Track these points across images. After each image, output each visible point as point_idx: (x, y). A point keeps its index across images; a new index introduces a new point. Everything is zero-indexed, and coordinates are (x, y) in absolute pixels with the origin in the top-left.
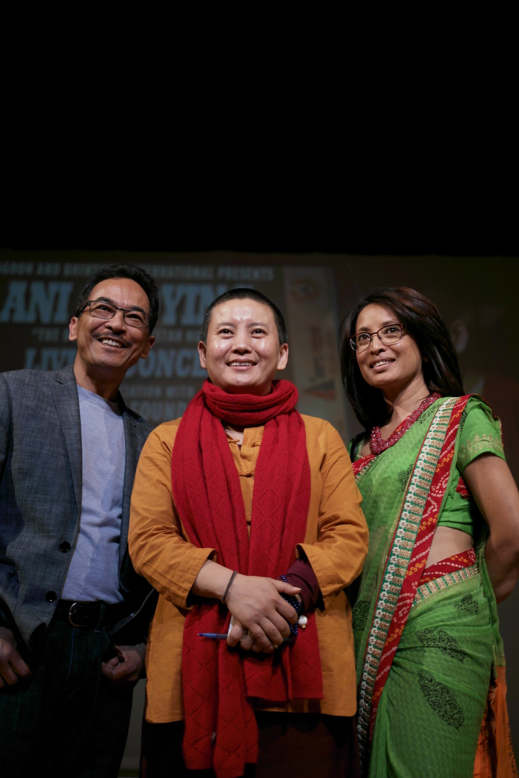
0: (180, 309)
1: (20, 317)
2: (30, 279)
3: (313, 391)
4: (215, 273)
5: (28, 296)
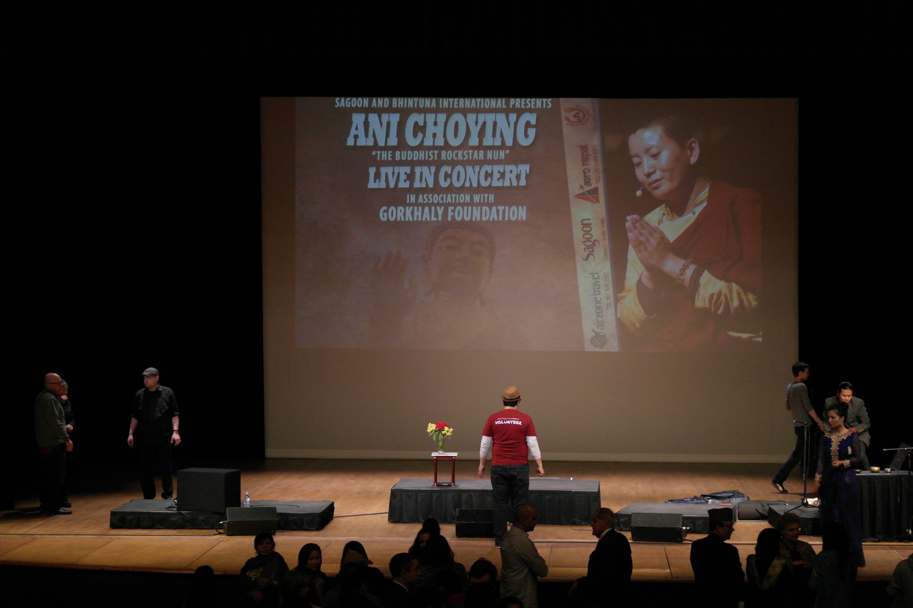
0: (482, 134)
1: (362, 142)
2: (367, 111)
3: (580, 196)
4: (507, 104)
5: (366, 124)
